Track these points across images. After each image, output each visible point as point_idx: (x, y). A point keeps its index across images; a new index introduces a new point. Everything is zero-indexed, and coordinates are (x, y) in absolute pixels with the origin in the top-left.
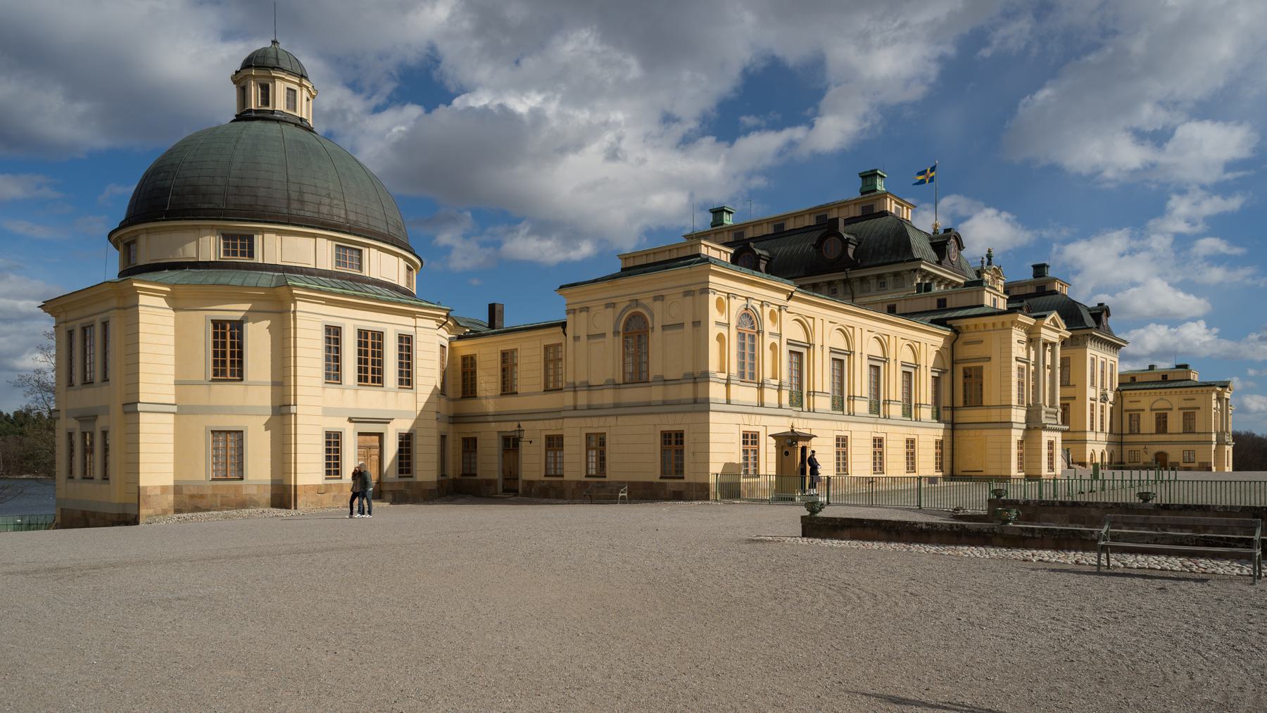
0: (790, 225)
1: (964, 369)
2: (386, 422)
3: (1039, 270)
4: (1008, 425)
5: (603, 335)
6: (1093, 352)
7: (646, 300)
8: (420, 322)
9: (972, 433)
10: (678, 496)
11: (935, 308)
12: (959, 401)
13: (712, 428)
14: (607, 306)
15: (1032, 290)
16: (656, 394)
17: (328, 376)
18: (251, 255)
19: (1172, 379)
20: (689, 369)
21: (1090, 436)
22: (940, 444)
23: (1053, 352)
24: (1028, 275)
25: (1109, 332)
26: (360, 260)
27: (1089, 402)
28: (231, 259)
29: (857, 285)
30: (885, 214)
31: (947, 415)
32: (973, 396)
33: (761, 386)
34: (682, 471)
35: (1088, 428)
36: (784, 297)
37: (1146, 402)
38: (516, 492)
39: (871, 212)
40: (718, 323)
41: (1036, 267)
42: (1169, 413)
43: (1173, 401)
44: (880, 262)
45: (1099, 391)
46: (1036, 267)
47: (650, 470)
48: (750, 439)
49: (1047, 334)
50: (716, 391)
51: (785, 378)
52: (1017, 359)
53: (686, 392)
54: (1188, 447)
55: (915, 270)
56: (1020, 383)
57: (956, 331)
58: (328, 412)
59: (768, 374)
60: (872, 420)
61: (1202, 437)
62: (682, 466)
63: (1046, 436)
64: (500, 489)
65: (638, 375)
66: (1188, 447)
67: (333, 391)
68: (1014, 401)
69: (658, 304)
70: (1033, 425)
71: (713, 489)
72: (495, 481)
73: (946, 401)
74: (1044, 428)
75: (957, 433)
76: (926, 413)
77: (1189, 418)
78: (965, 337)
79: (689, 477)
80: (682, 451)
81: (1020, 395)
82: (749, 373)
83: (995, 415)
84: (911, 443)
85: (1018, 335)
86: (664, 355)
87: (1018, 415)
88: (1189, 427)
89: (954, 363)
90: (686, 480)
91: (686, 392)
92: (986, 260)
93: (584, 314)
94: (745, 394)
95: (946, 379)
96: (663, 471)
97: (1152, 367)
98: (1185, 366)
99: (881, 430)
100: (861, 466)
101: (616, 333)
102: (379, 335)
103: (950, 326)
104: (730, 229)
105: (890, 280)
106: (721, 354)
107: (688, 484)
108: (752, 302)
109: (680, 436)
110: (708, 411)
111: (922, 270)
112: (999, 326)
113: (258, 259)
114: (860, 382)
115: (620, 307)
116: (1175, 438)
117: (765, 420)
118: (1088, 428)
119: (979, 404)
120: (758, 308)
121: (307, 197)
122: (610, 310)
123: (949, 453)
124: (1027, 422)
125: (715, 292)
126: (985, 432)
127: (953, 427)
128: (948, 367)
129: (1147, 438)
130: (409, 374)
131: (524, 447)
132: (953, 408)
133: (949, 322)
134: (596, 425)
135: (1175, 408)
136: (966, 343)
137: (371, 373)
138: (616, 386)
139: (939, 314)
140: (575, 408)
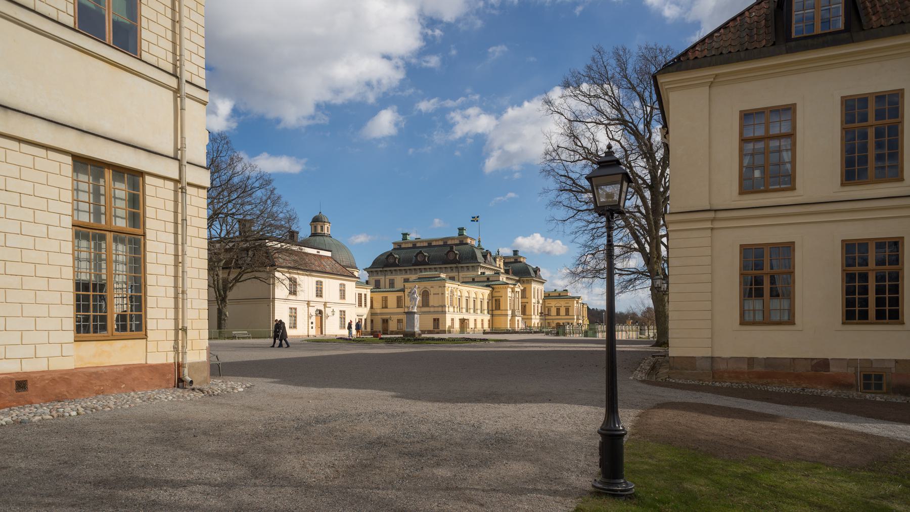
0: (434, 244)
3: (515, 252)
4: (507, 315)
6: (535, 286)
15: (512, 260)
16: (432, 309)
19: (562, 295)
21: (533, 317)
25: (540, 277)
30: (467, 244)
32: (498, 307)
37: (553, 304)
39: (462, 243)
43: (562, 303)
49: (517, 289)
53: (440, 309)
63: (517, 318)
70: (513, 315)
76: (486, 312)
77: (567, 310)
82: (452, 305)
83: (503, 312)
85: (509, 290)
86: (433, 300)
87: (510, 312)
91: (440, 309)
94: (451, 309)
99: (475, 317)
100: (479, 326)
104: (410, 242)
106: (447, 302)
114: (471, 305)
123: (491, 322)
127: (492, 315)
131: (390, 322)
139: (487, 282)
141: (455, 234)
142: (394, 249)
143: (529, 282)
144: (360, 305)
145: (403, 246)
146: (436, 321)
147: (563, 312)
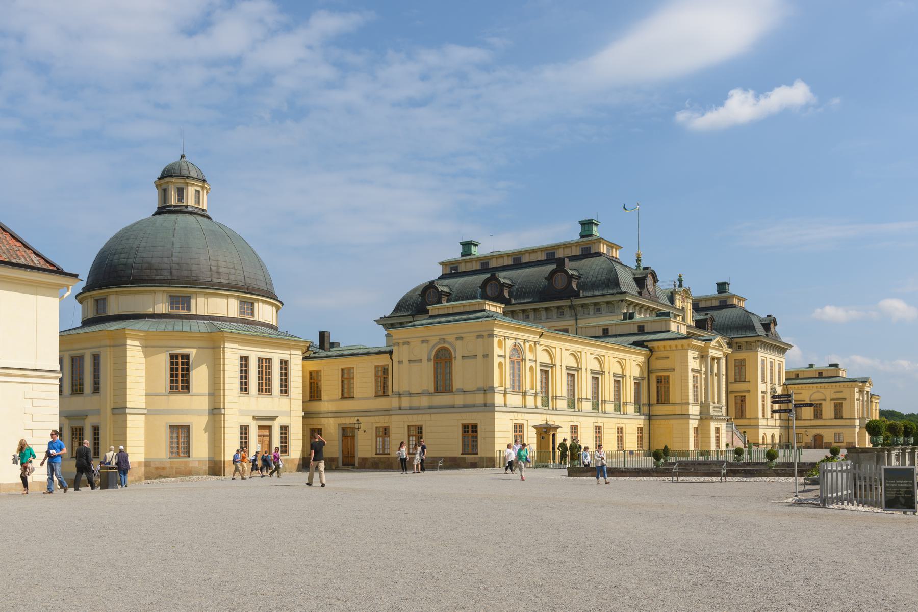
0: (526, 259)
2: (273, 419)
3: (722, 287)
4: (686, 416)
5: (420, 360)
6: (764, 356)
7: (451, 339)
8: (293, 352)
9: (663, 422)
10: (474, 465)
11: (636, 331)
14: (423, 342)
15: (716, 303)
16: (459, 400)
17: (241, 389)
18: (189, 310)
19: (827, 376)
20: (482, 385)
21: (762, 422)
22: (640, 430)
23: (718, 363)
24: (713, 291)
25: (776, 338)
26: (253, 310)
27: (760, 395)
28: (175, 312)
29: (579, 309)
30: (599, 254)
31: (645, 409)
32: (663, 396)
33: (524, 395)
34: (477, 449)
35: (760, 415)
38: (353, 465)
39: (588, 253)
41: (719, 285)
42: (823, 402)
43: (825, 394)
45: (769, 386)
46: (719, 285)
47: (455, 449)
49: (713, 353)
50: (498, 399)
51: (539, 388)
52: (693, 370)
53: (479, 399)
54: (838, 430)
55: (622, 301)
56: (695, 387)
58: (242, 413)
59: (528, 387)
61: (848, 422)
62: (476, 446)
63: (713, 425)
64: (340, 463)
66: (838, 430)
67: (244, 398)
68: (691, 400)
69: (459, 343)
70: (705, 417)
71: (497, 461)
72: (337, 458)
73: (644, 399)
74: (712, 418)
75: (652, 422)
76: (631, 409)
78: (656, 354)
79: (482, 452)
80: (476, 437)
81: (695, 395)
82: (518, 388)
83: (678, 410)
84: (620, 430)
85: (692, 354)
86: (462, 374)
87: (694, 410)
88: (838, 414)
90: (479, 455)
92: (678, 283)
93: (406, 346)
94: (515, 400)
95: (644, 384)
96: (463, 449)
97: (811, 366)
98: (836, 366)
99: (600, 421)
101: (429, 360)
102: (269, 361)
103: (647, 347)
104: (477, 259)
105: (604, 308)
106: (501, 377)
107: (481, 458)
108: (519, 341)
110: (494, 411)
111: (627, 301)
112: (680, 347)
113: (193, 312)
114: (585, 388)
115: (432, 343)
116: (828, 423)
118: (760, 415)
119: (667, 402)
120: (522, 344)
121: (222, 270)
122: (425, 345)
123: (647, 435)
124: (701, 414)
126: (672, 422)
127: (650, 417)
128: (646, 375)
129: (808, 423)
130: (286, 386)
132: (649, 405)
133: (645, 344)
134: (416, 420)
135: (828, 399)
136: (657, 358)
137: (265, 388)
138: (430, 394)
140: (400, 409)
141: (573, 234)
142: (444, 277)
143: (751, 347)
144: (265, 388)
145: (462, 268)
146: (470, 431)
147: (828, 410)
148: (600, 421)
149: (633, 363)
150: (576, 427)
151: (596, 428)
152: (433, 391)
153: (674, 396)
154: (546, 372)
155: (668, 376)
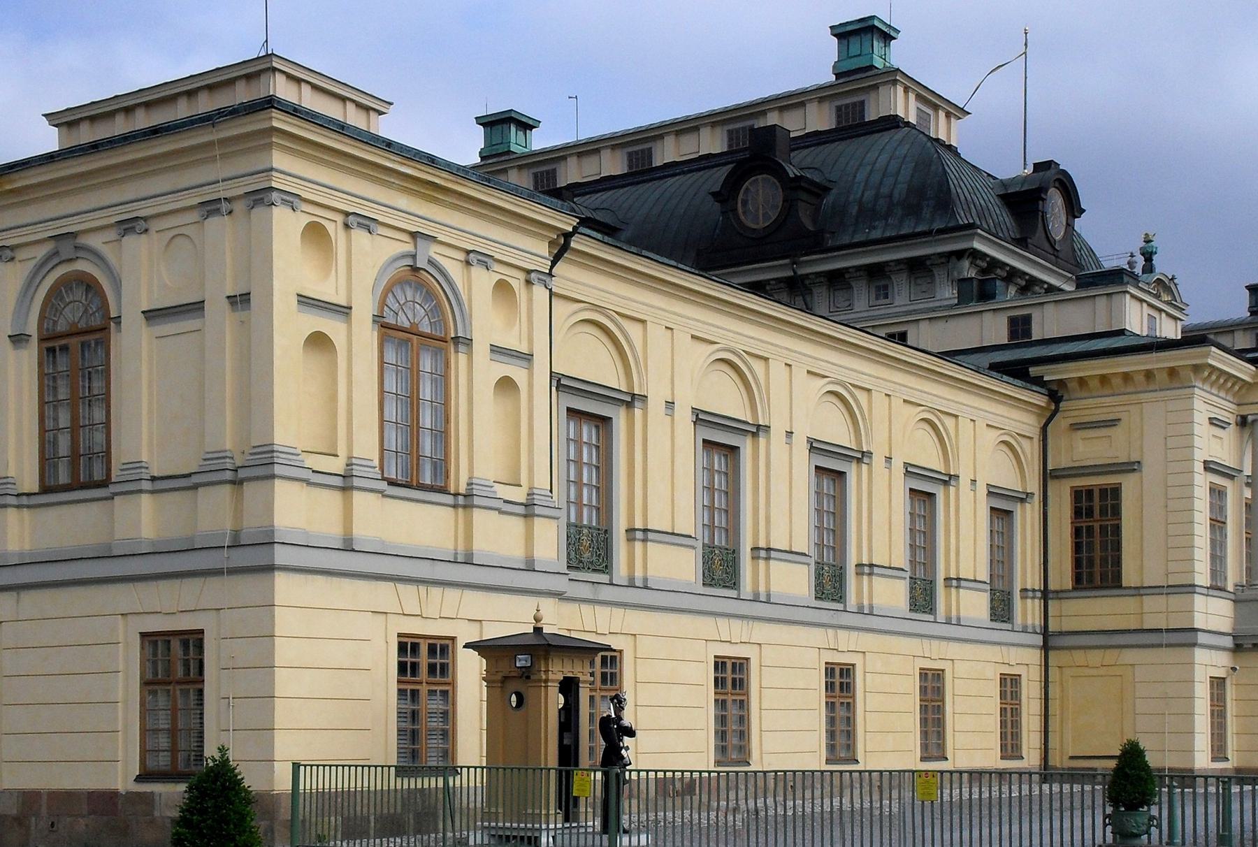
1: (1077, 494)
9: (1095, 657)
12: (1062, 576)
13: (284, 621)
22: (1010, 685)
30: (892, 123)
31: (1028, 612)
36: (543, 249)
40: (306, 301)
44: (876, 234)
48: (423, 663)
51: (542, 482)
52: (1208, 467)
53: (213, 512)
55: (959, 254)
56: (1218, 524)
57: (1055, 394)
60: (824, 617)
65: (77, 464)
68: (1202, 576)
73: (1027, 573)
83: (1156, 612)
89: (1048, 476)
92: (1140, 261)
95: (1027, 519)
103: (1038, 381)
109: (193, 641)
117: (475, 604)
120: (454, 269)
125: (292, 201)
126: (1129, 656)
127: (1049, 641)
128: (1034, 486)
132: (1046, 594)
133: (1034, 371)
136: (1077, 427)
146: (175, 665)
148: (849, 647)
149: (986, 435)
150: (740, 665)
151: (830, 670)
152: (30, 482)
153: (1137, 563)
154: (593, 414)
155: (1116, 491)
